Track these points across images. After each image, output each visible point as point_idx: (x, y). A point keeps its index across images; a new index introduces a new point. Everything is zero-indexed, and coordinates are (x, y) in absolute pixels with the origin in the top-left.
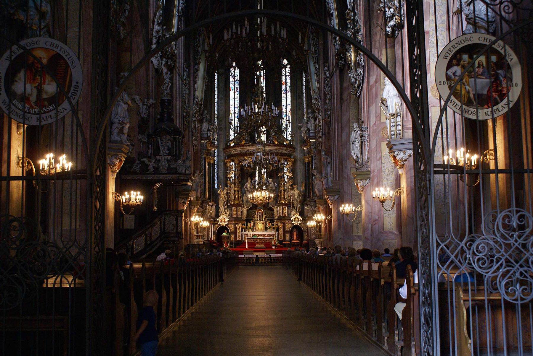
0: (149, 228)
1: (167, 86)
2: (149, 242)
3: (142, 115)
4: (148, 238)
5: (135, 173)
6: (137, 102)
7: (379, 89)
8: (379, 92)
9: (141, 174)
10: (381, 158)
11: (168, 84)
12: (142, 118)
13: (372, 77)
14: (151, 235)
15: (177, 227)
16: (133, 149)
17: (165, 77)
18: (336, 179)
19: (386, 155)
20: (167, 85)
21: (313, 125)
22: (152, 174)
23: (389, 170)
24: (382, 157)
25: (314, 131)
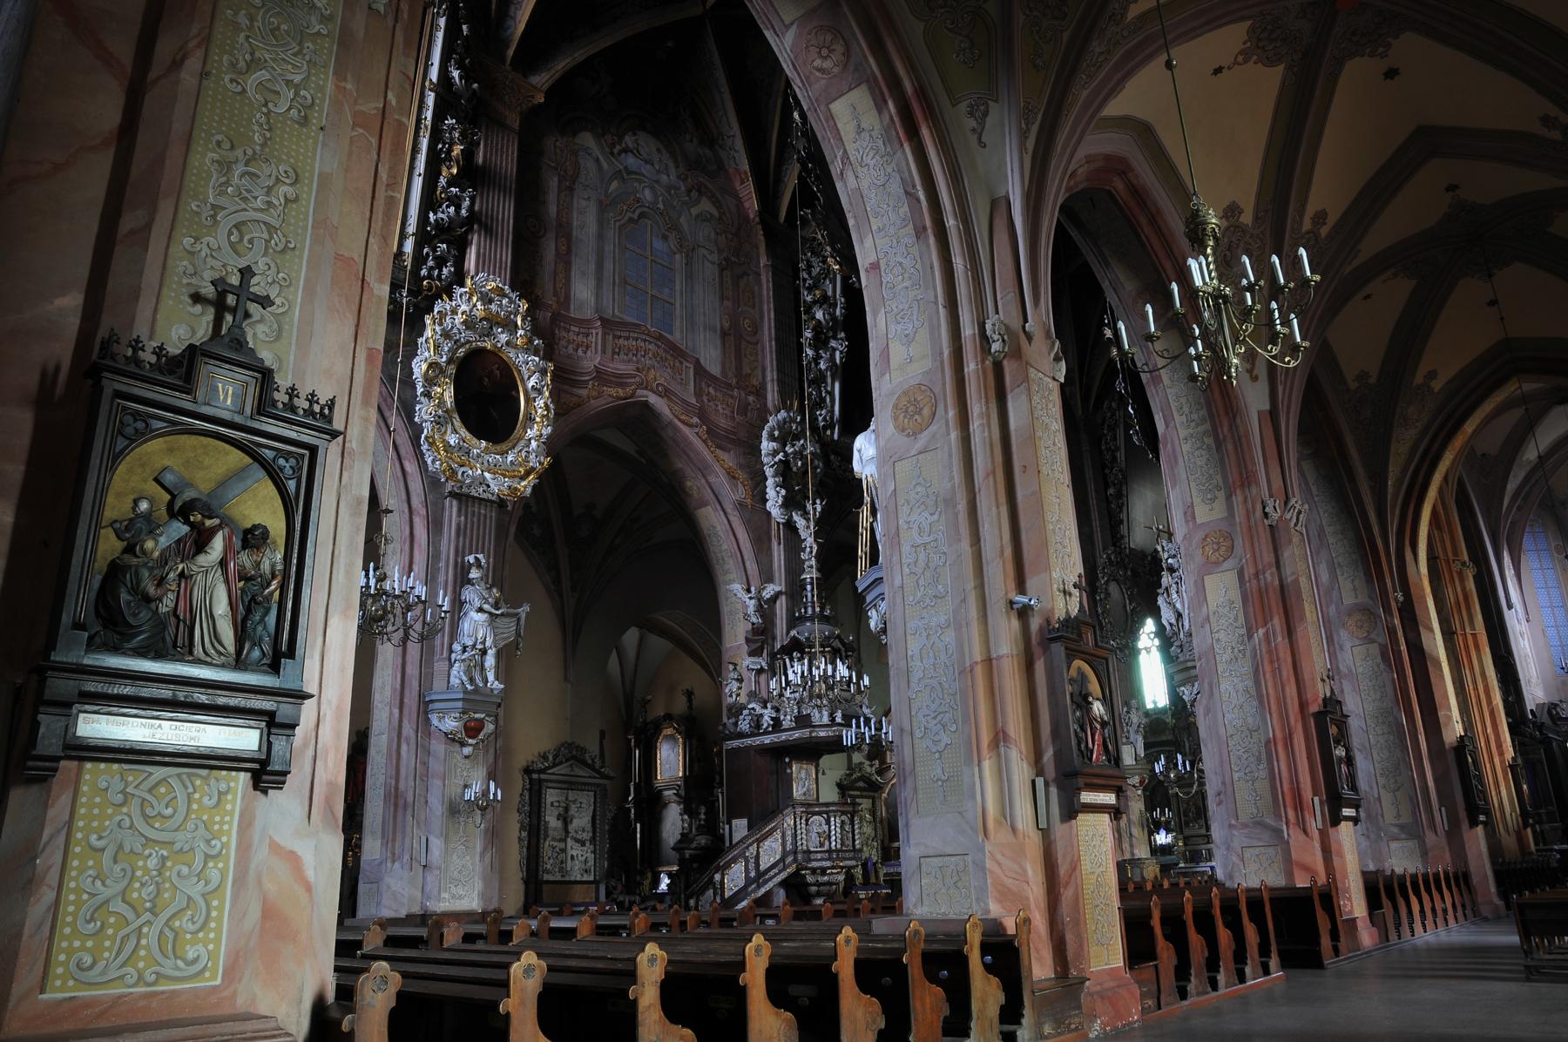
0: (751, 844)
1: (811, 552)
2: (753, 874)
3: (754, 620)
4: (752, 866)
5: (742, 735)
7: (1177, 442)
8: (1178, 450)
9: (753, 735)
10: (1208, 619)
11: (811, 547)
12: (753, 624)
14: (757, 857)
15: (830, 837)
16: (740, 688)
17: (803, 535)
19: (1220, 609)
20: (808, 549)
22: (770, 733)
23: (1233, 648)
24: (1211, 617)
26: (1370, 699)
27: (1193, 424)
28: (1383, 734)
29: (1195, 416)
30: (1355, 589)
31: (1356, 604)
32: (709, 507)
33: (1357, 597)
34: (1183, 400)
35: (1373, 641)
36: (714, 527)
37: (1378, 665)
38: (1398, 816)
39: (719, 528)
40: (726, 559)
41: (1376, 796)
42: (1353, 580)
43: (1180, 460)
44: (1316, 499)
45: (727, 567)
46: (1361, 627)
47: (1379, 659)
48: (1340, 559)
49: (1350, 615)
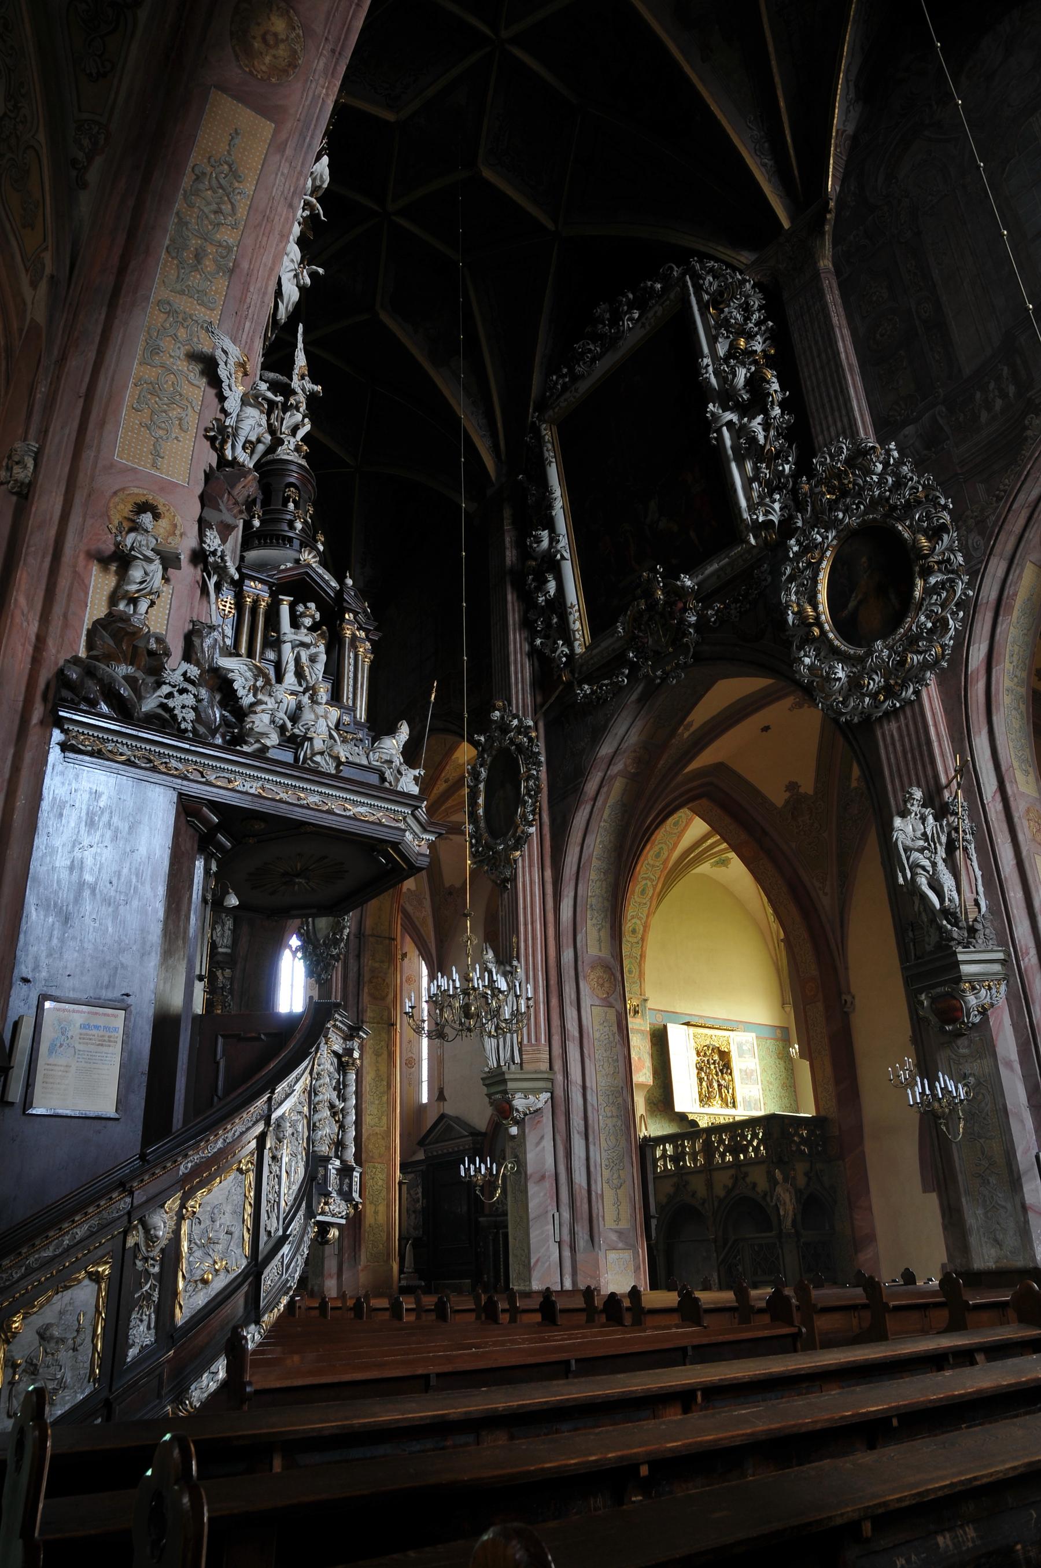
6: (222, 372)
13: (976, 645)
18: (537, 1039)
21: (228, 933)
25: (228, 951)
26: (604, 1072)
27: (1016, 680)
28: (612, 1117)
29: (1018, 673)
30: (600, 941)
31: (600, 958)
32: (268, 128)
33: (600, 950)
34: (1016, 648)
35: (611, 1006)
36: (235, 174)
37: (614, 1035)
38: (618, 1220)
39: (249, 187)
40: (209, 265)
41: (599, 1192)
42: (599, 930)
43: (1002, 709)
44: (602, 824)
45: (195, 280)
46: (602, 985)
47: (615, 1029)
48: (594, 901)
49: (593, 968)
